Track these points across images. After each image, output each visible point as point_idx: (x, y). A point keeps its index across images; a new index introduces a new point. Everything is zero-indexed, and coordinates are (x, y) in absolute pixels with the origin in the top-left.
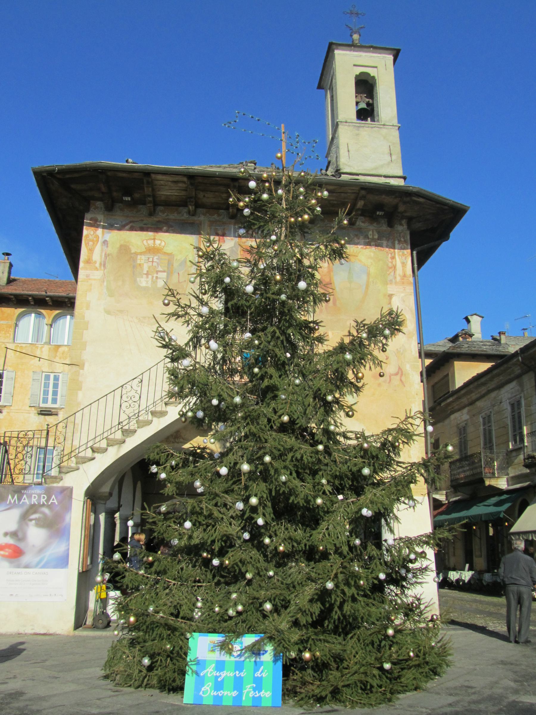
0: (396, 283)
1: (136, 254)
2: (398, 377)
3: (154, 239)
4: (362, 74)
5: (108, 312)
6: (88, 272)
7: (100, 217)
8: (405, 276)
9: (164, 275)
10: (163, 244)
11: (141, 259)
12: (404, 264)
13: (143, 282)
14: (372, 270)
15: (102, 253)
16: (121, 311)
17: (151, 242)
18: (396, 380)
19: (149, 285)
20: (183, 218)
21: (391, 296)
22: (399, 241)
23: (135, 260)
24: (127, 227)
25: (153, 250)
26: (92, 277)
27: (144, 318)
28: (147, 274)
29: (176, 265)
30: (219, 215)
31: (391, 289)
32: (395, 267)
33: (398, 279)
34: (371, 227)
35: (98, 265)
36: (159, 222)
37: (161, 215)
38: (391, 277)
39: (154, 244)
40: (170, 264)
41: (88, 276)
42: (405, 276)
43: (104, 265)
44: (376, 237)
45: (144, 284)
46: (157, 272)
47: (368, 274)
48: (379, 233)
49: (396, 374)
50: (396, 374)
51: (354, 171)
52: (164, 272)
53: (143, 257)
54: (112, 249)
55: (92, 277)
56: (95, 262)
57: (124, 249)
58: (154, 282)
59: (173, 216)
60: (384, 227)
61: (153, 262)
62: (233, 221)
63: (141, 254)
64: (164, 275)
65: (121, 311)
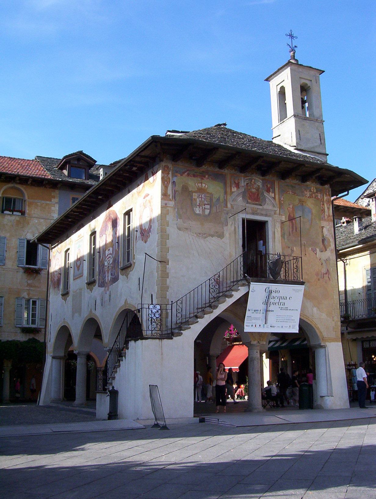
0: (325, 220)
1: (193, 192)
2: (327, 275)
3: (201, 183)
4: (303, 83)
5: (179, 229)
6: (166, 202)
7: (170, 166)
8: (329, 216)
9: (208, 207)
10: (207, 186)
11: (195, 196)
12: (328, 208)
13: (198, 211)
14: (314, 211)
15: (172, 190)
16: (187, 229)
17: (200, 185)
18: (326, 277)
19: (201, 213)
20: (216, 170)
21: (323, 227)
22: (326, 194)
23: (192, 196)
24: (186, 174)
25: (201, 191)
26: (168, 205)
27: (200, 234)
28: (199, 206)
29: (214, 200)
30: (236, 170)
31: (324, 223)
32: (323, 211)
33: (326, 217)
34: (313, 185)
35: (171, 197)
36: (203, 172)
37: (204, 168)
38: (322, 216)
39: (202, 186)
40: (211, 200)
41: (166, 204)
42: (329, 216)
43: (174, 197)
44: (315, 191)
45: (198, 212)
46: (205, 205)
47: (312, 214)
48: (316, 188)
49: (326, 274)
50: (326, 274)
51: (302, 148)
52: (208, 204)
53: (196, 194)
54: (178, 188)
55: (168, 205)
56: (169, 195)
57: (185, 189)
58: (203, 211)
59: (211, 169)
60: (319, 186)
61: (202, 198)
62: (243, 174)
63: (195, 192)
64: (208, 207)
65: (187, 229)
